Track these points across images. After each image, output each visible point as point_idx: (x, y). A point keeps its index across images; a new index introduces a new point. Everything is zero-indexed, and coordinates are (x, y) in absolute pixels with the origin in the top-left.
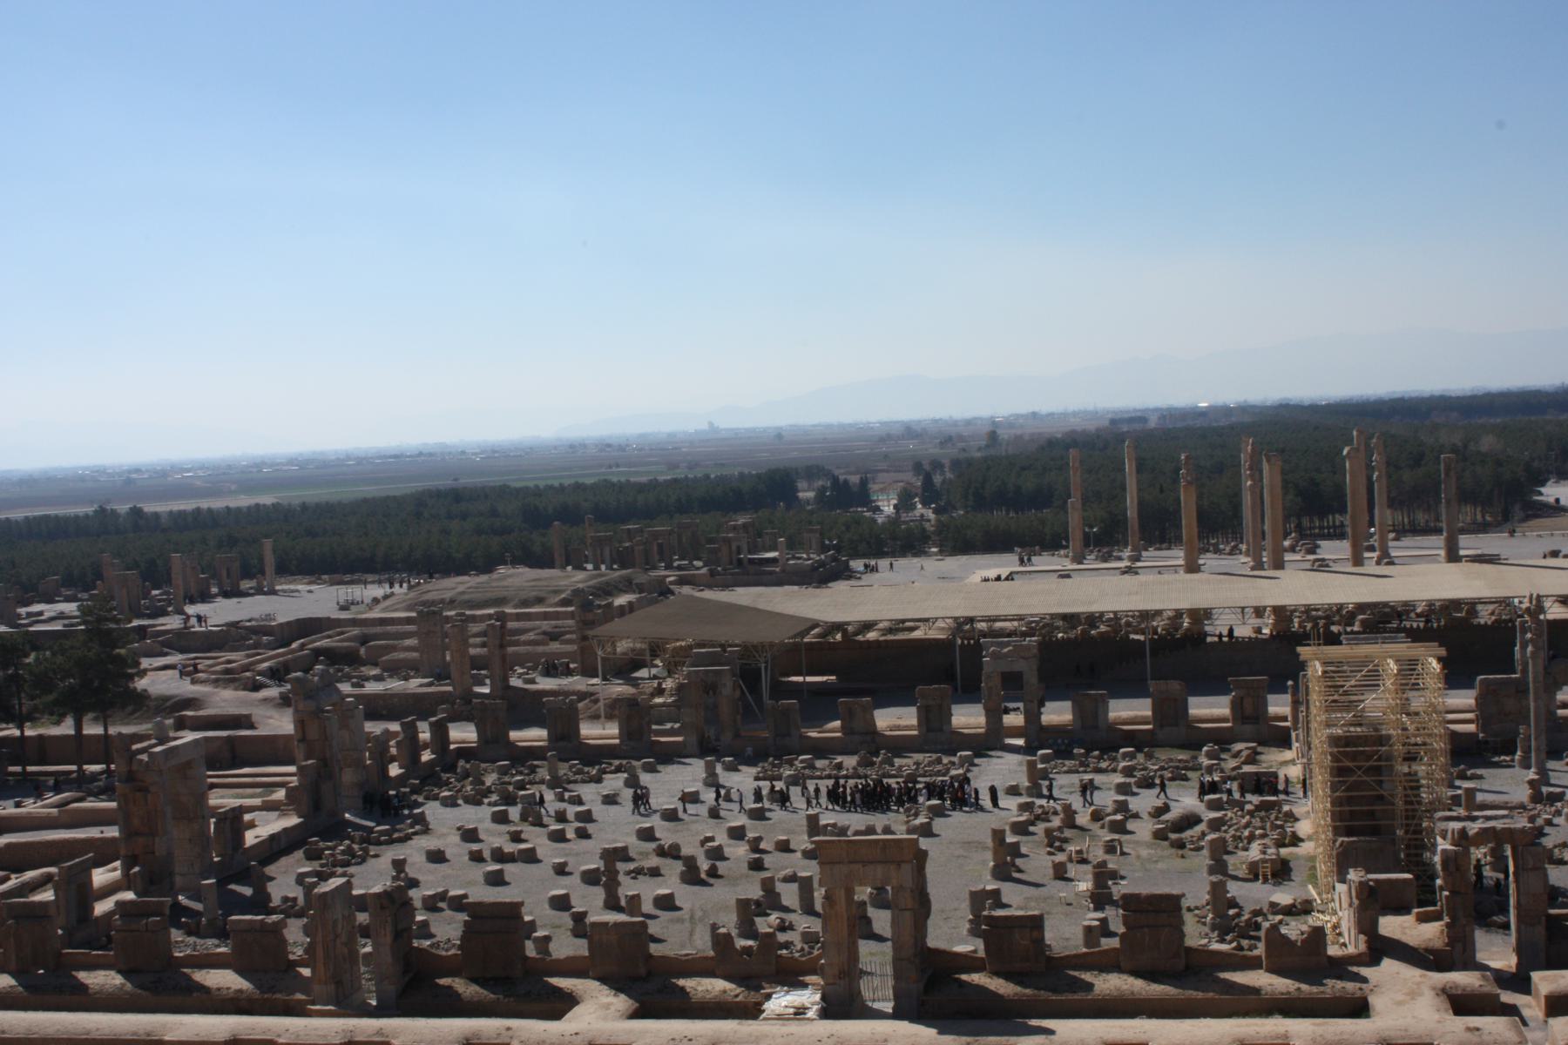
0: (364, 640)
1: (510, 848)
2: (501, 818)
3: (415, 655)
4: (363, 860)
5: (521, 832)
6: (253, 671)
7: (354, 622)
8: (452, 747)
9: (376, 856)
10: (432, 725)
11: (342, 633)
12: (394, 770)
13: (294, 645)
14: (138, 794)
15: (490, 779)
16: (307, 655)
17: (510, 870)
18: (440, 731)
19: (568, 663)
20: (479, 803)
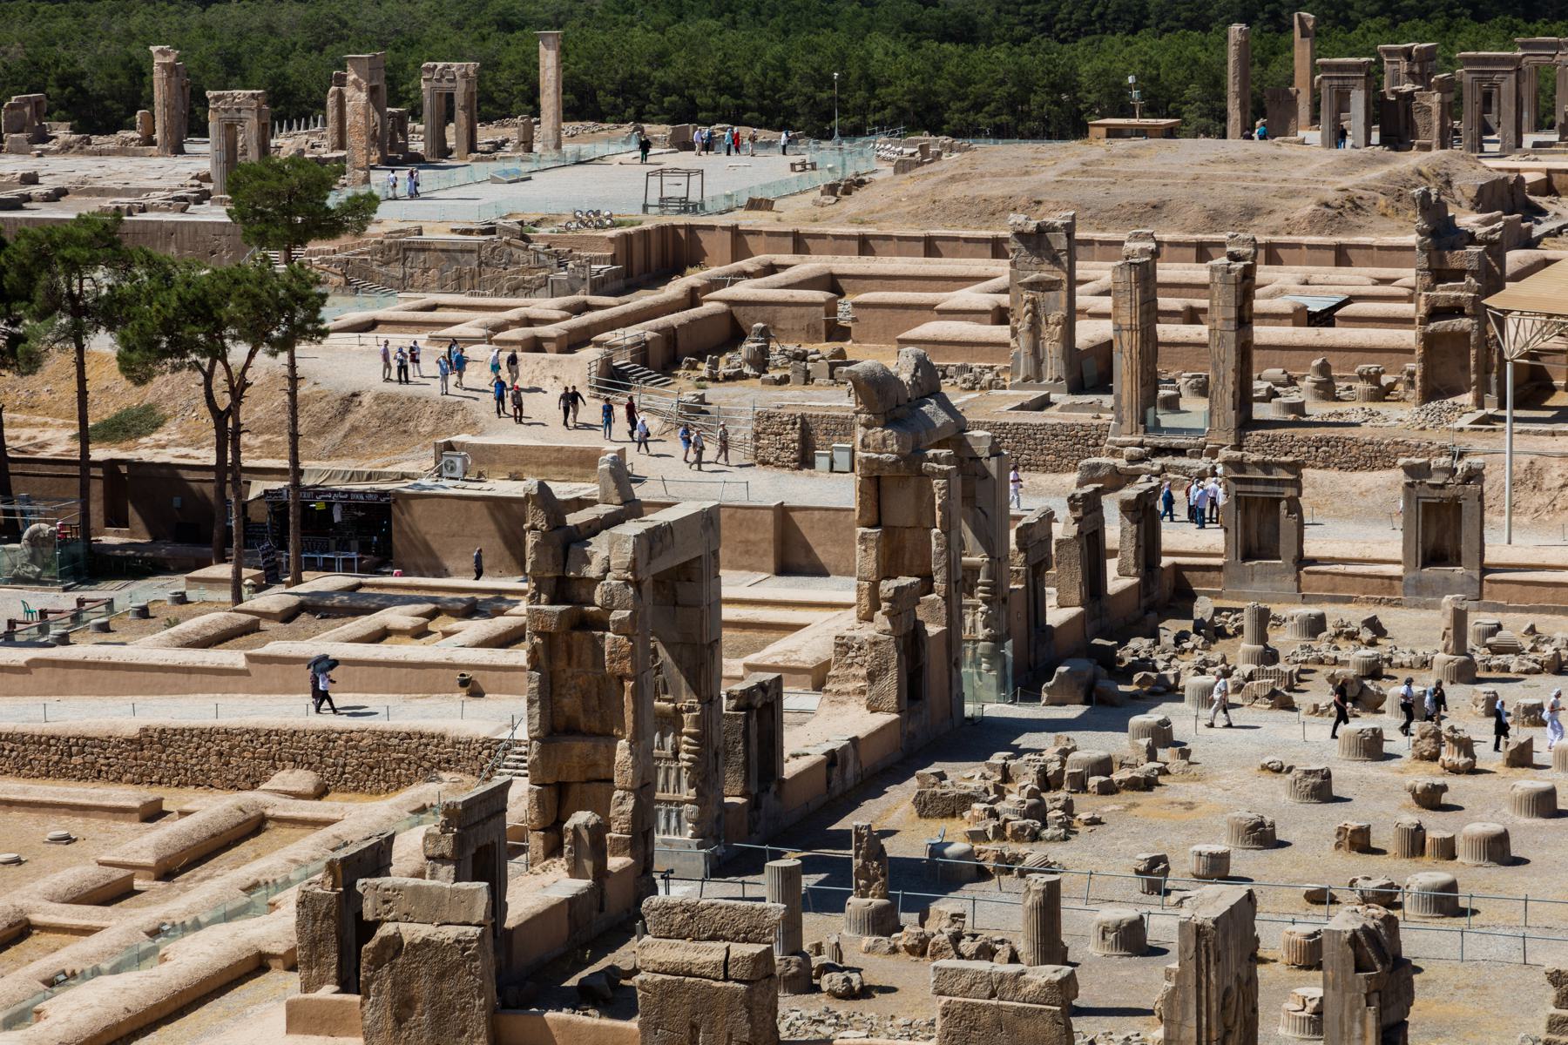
0: (832, 283)
1: (1437, 826)
2: (1372, 747)
3: (1001, 333)
4: (1068, 831)
5: (1444, 788)
6: (599, 344)
7: (799, 242)
8: (1166, 561)
9: (1095, 822)
10: (1127, 507)
11: (771, 269)
12: (1056, 616)
13: (675, 289)
14: (576, 634)
15: (1284, 639)
16: (711, 317)
17: (1471, 875)
18: (1145, 515)
19: (1378, 374)
20: (1289, 706)
